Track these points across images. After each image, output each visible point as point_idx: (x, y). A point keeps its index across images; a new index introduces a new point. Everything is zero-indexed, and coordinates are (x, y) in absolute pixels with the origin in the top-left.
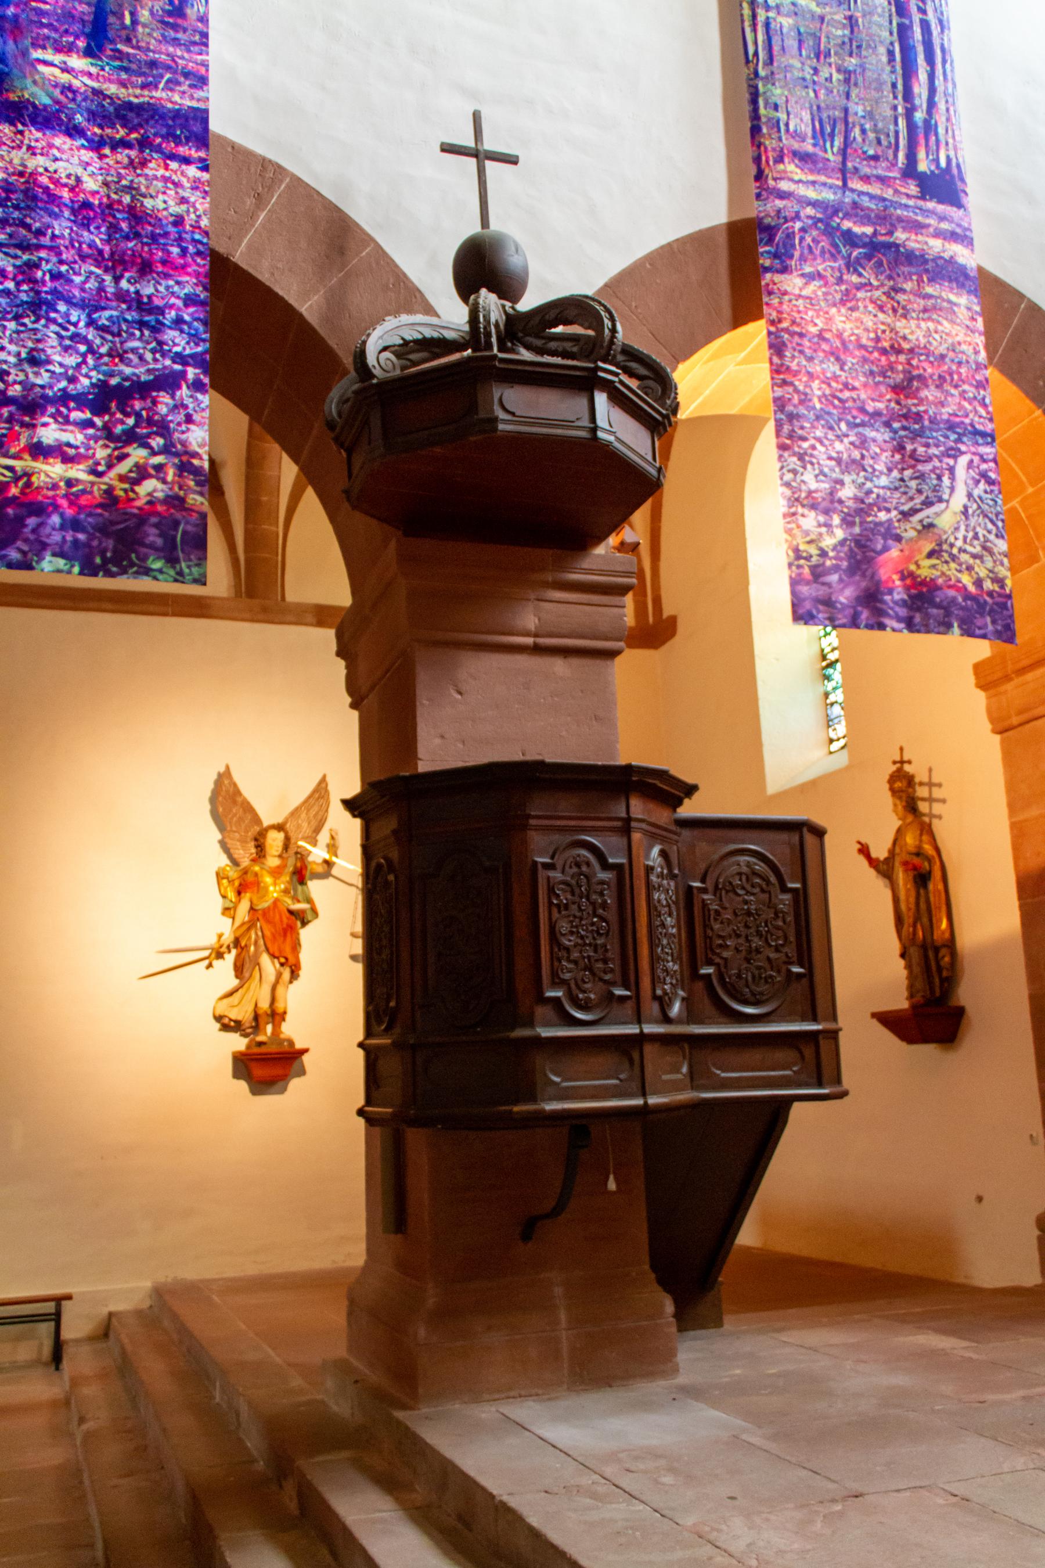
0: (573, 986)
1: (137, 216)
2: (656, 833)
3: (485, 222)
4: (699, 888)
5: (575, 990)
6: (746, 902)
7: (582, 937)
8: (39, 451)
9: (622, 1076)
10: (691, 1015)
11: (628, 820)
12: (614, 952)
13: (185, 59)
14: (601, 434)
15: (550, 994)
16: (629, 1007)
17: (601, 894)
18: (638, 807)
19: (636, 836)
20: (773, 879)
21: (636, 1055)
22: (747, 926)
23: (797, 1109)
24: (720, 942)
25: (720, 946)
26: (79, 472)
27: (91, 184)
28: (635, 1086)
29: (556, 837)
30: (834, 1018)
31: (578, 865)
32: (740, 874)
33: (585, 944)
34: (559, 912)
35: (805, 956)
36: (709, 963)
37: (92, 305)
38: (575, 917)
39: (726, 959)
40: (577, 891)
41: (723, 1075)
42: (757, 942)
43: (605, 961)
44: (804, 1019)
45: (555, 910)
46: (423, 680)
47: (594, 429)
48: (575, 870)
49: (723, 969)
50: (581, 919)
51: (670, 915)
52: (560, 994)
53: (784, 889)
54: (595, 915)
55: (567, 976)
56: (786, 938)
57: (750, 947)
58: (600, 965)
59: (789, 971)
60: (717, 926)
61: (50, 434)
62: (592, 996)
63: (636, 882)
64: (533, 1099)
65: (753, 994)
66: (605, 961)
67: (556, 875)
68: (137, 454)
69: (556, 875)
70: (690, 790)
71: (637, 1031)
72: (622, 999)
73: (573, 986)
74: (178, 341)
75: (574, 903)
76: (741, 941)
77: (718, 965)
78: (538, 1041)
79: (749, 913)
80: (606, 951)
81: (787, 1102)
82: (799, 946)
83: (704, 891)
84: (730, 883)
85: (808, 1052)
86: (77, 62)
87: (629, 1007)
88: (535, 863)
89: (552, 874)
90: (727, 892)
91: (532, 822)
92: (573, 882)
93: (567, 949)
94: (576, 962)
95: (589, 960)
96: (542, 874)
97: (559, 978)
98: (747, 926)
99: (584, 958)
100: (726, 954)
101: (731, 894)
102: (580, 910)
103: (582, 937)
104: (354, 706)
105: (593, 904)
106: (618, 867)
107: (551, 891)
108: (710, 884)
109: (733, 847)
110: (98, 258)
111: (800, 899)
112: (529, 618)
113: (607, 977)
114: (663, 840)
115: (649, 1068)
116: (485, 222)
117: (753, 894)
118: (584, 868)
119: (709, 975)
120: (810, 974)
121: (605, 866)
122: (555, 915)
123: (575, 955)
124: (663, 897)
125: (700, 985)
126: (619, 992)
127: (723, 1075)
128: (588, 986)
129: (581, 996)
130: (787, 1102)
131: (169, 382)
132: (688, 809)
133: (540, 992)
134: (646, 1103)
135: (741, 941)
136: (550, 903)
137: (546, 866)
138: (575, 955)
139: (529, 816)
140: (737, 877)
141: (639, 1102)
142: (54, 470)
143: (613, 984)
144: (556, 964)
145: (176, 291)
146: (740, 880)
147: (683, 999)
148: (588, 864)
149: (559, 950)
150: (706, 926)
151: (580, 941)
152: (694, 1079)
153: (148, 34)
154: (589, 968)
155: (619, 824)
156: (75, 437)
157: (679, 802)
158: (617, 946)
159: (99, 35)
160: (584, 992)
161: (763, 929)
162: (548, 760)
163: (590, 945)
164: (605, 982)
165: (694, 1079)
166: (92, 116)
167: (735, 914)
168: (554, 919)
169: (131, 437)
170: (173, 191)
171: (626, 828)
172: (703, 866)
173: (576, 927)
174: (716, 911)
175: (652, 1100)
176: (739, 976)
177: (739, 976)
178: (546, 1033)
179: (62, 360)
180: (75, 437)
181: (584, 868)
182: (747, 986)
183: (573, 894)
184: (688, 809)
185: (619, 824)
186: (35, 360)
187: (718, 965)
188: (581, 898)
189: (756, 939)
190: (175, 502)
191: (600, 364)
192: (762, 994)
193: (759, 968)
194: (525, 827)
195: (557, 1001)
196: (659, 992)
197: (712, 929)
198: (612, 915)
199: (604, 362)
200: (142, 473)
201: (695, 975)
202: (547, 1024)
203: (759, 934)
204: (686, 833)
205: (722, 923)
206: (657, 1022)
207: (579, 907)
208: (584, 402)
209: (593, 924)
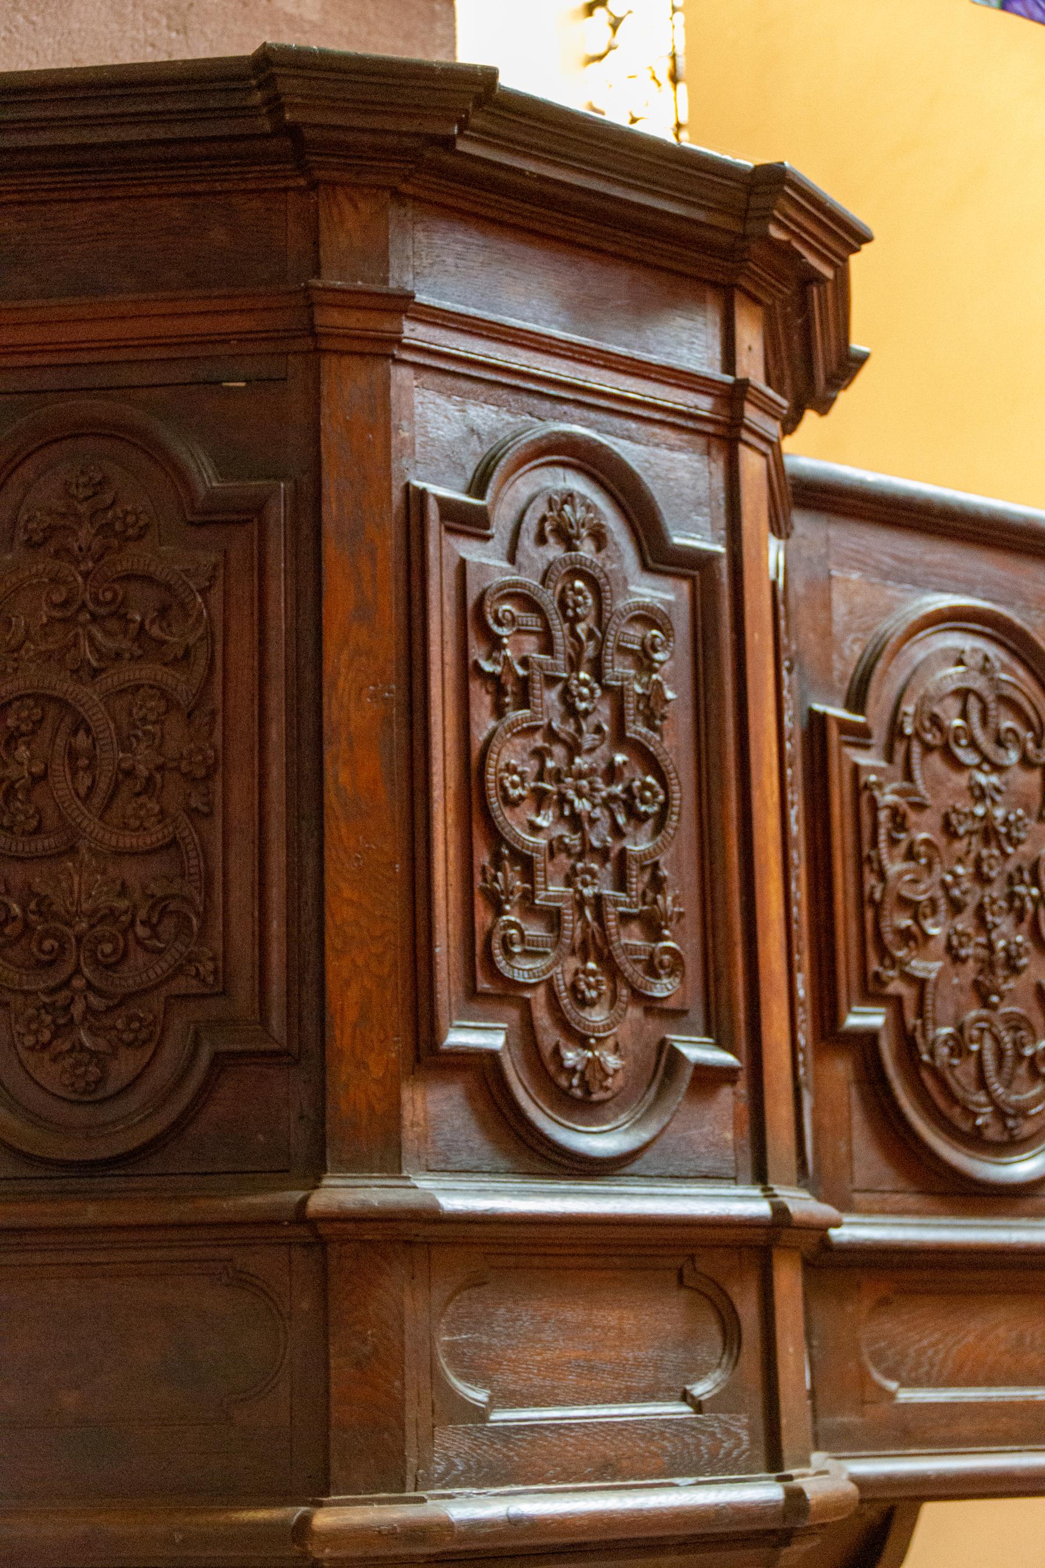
0: (542, 1017)
4: (845, 727)
5: (549, 1036)
6: (979, 794)
7: (575, 821)
9: (701, 1389)
12: (678, 899)
15: (459, 1037)
16: (719, 1120)
17: (644, 661)
21: (748, 1310)
22: (982, 879)
24: (906, 922)
25: (906, 936)
28: (742, 1429)
29: (489, 417)
33: (587, 850)
34: (499, 711)
36: (872, 992)
38: (552, 735)
39: (921, 984)
40: (560, 630)
41: (906, 1395)
42: (1008, 933)
43: (654, 932)
45: (482, 700)
48: (554, 551)
49: (911, 1020)
50: (574, 749)
52: (495, 1041)
54: (620, 739)
55: (522, 969)
57: (990, 946)
58: (633, 937)
60: (894, 867)
62: (612, 1061)
64: (391, 1477)
65: (1000, 1114)
66: (653, 926)
67: (486, 559)
69: (486, 559)
71: (762, 1208)
72: (708, 1079)
73: (542, 1017)
75: (551, 681)
76: (964, 923)
77: (896, 1003)
79: (988, 834)
80: (657, 884)
83: (860, 736)
84: (935, 720)
87: (719, 1120)
88: (416, 499)
89: (471, 551)
90: (928, 749)
91: (414, 332)
92: (548, 599)
93: (527, 865)
94: (553, 919)
95: (600, 916)
96: (447, 549)
97: (494, 974)
98: (982, 879)
99: (580, 903)
100: (927, 966)
101: (936, 760)
102: (571, 712)
103: (575, 821)
105: (617, 696)
106: (689, 566)
107: (474, 619)
108: (876, 718)
117: (998, 768)
118: (586, 549)
119: (870, 1037)
121: (657, 555)
122: (484, 724)
123: (553, 890)
125: (841, 1070)
126: (698, 1051)
127: (906, 1395)
128: (597, 1016)
129: (571, 1056)
134: (796, 1496)
135: (964, 923)
136: (467, 671)
138: (553, 890)
139: (403, 304)
140: (954, 705)
141: (764, 1492)
143: (675, 1015)
144: (483, 917)
146: (964, 715)
148: (599, 537)
149: (497, 861)
150: (864, 862)
151: (572, 840)
154: (596, 947)
155: (703, 404)
158: (691, 875)
160: (582, 1042)
162: (512, 79)
163: (603, 854)
164: (651, 1006)
167: (948, 829)
168: (479, 736)
172: (852, 651)
173: (557, 776)
174: (895, 812)
176: (958, 1045)
178: (459, 1198)
181: (586, 549)
182: (982, 1083)
183: (548, 647)
185: (703, 404)
187: (896, 1003)
188: (574, 665)
189: (1005, 923)
192: (1021, 1112)
193: (1016, 1023)
194: (385, 349)
195: (482, 1066)
197: (882, 875)
198: (674, 744)
202: (446, 1167)
205: (911, 855)
207: (567, 697)
209: (612, 773)
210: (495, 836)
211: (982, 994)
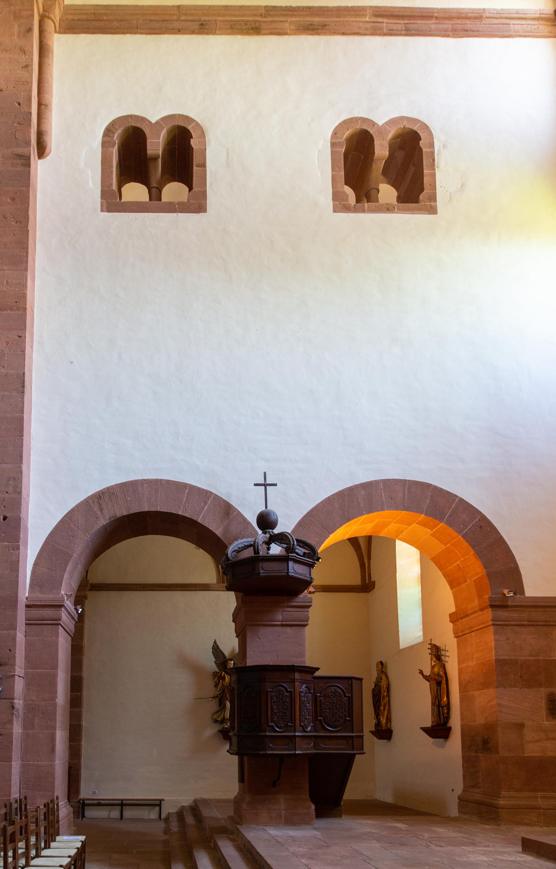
2: (303, 682)
3: (266, 507)
10: (315, 729)
11: (294, 679)
14: (290, 574)
15: (270, 724)
18: (297, 676)
19: (296, 683)
20: (342, 693)
23: (357, 756)
30: (362, 732)
31: (279, 691)
32: (332, 692)
35: (351, 714)
44: (349, 732)
46: (249, 635)
47: (288, 573)
51: (309, 703)
53: (345, 696)
56: (345, 710)
59: (346, 719)
63: (296, 696)
64: (265, 750)
67: (273, 694)
70: (318, 669)
72: (291, 726)
78: (266, 736)
81: (355, 754)
82: (349, 712)
85: (350, 742)
93: (276, 713)
94: (278, 716)
104: (237, 636)
107: (272, 697)
109: (330, 684)
111: (350, 699)
112: (279, 617)
113: (287, 720)
114: (307, 683)
115: (297, 744)
116: (266, 507)
120: (352, 721)
121: (287, 691)
124: (306, 699)
125: (318, 722)
130: (355, 754)
132: (317, 674)
133: (268, 723)
137: (270, 691)
141: (294, 752)
143: (288, 722)
147: (312, 726)
148: (282, 691)
152: (315, 747)
157: (315, 672)
161: (338, 707)
165: (315, 747)
171: (293, 681)
175: (297, 752)
177: (330, 720)
178: (268, 734)
184: (317, 674)
191: (290, 554)
195: (273, 726)
196: (302, 724)
199: (291, 553)
201: (317, 720)
202: (269, 732)
203: (337, 708)
204: (316, 681)
206: (301, 732)
208: (286, 565)
210: (274, 712)
211: (333, 716)
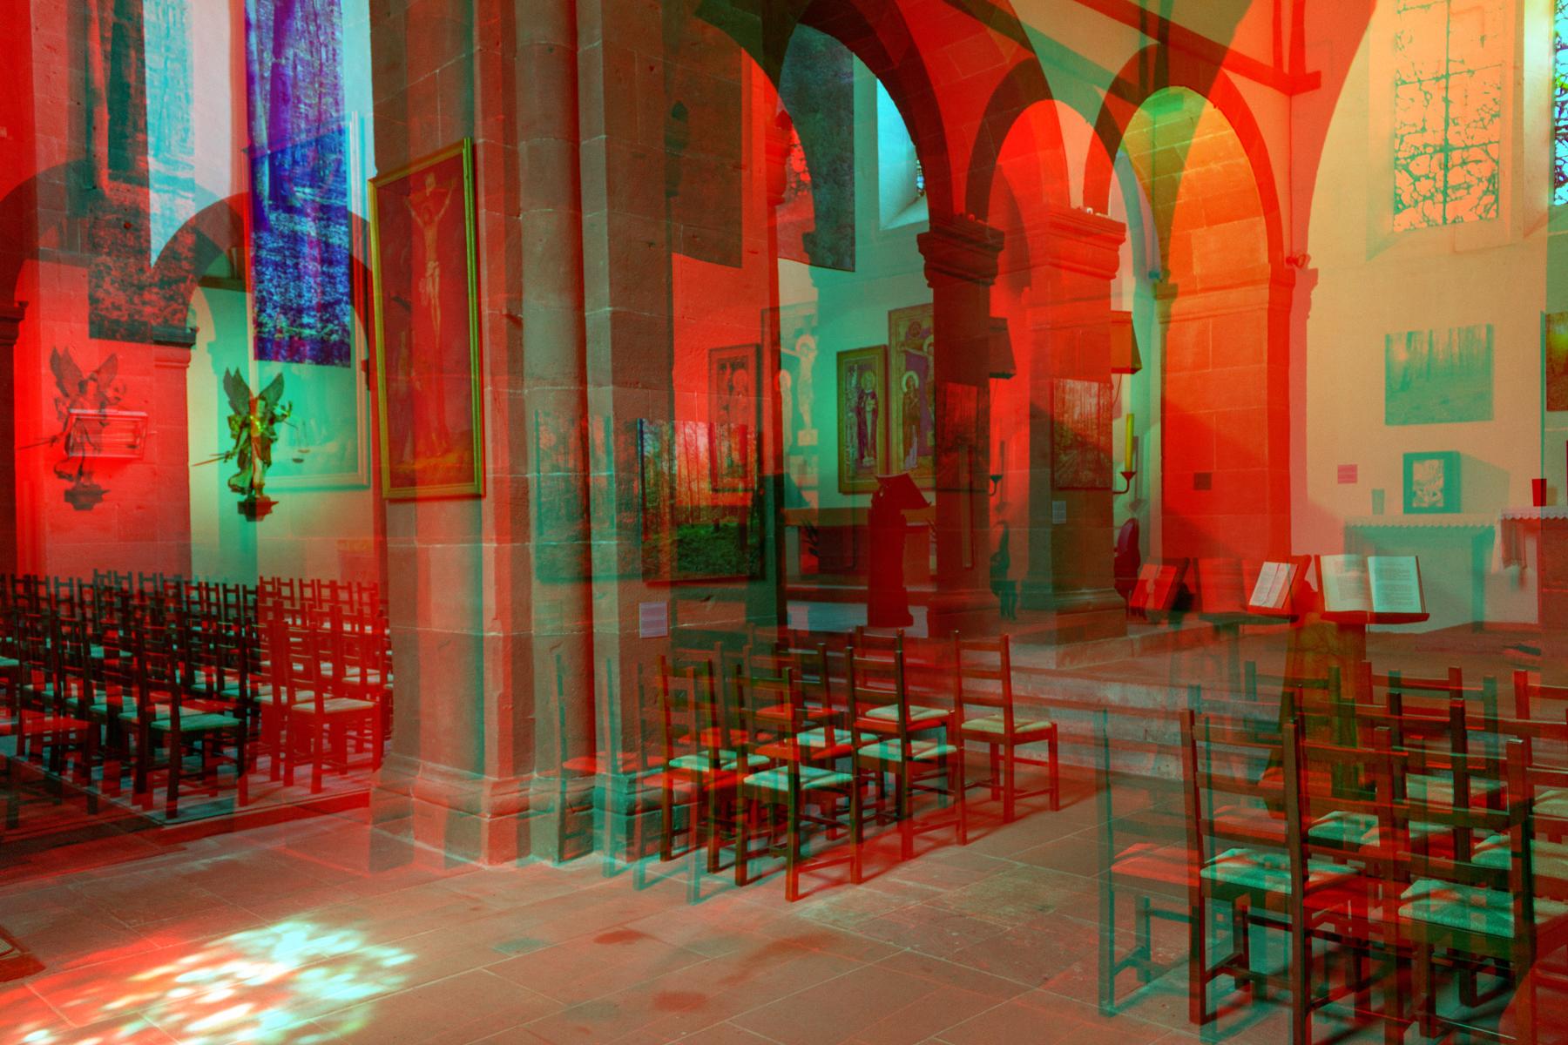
1: (328, 245)
8: (303, 326)
13: (340, 188)
26: (313, 332)
27: (313, 234)
37: (315, 276)
61: (306, 320)
68: (330, 326)
74: (341, 289)
86: (307, 190)
110: (314, 259)
131: (338, 302)
142: (307, 332)
145: (340, 271)
153: (330, 180)
156: (312, 321)
159: (315, 179)
166: (315, 210)
169: (328, 321)
170: (339, 236)
179: (307, 295)
180: (312, 321)
186: (300, 296)
190: (342, 342)
200: (332, 332)
